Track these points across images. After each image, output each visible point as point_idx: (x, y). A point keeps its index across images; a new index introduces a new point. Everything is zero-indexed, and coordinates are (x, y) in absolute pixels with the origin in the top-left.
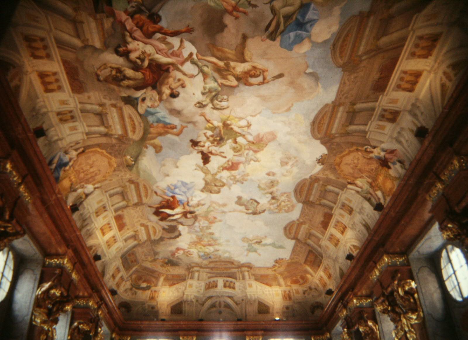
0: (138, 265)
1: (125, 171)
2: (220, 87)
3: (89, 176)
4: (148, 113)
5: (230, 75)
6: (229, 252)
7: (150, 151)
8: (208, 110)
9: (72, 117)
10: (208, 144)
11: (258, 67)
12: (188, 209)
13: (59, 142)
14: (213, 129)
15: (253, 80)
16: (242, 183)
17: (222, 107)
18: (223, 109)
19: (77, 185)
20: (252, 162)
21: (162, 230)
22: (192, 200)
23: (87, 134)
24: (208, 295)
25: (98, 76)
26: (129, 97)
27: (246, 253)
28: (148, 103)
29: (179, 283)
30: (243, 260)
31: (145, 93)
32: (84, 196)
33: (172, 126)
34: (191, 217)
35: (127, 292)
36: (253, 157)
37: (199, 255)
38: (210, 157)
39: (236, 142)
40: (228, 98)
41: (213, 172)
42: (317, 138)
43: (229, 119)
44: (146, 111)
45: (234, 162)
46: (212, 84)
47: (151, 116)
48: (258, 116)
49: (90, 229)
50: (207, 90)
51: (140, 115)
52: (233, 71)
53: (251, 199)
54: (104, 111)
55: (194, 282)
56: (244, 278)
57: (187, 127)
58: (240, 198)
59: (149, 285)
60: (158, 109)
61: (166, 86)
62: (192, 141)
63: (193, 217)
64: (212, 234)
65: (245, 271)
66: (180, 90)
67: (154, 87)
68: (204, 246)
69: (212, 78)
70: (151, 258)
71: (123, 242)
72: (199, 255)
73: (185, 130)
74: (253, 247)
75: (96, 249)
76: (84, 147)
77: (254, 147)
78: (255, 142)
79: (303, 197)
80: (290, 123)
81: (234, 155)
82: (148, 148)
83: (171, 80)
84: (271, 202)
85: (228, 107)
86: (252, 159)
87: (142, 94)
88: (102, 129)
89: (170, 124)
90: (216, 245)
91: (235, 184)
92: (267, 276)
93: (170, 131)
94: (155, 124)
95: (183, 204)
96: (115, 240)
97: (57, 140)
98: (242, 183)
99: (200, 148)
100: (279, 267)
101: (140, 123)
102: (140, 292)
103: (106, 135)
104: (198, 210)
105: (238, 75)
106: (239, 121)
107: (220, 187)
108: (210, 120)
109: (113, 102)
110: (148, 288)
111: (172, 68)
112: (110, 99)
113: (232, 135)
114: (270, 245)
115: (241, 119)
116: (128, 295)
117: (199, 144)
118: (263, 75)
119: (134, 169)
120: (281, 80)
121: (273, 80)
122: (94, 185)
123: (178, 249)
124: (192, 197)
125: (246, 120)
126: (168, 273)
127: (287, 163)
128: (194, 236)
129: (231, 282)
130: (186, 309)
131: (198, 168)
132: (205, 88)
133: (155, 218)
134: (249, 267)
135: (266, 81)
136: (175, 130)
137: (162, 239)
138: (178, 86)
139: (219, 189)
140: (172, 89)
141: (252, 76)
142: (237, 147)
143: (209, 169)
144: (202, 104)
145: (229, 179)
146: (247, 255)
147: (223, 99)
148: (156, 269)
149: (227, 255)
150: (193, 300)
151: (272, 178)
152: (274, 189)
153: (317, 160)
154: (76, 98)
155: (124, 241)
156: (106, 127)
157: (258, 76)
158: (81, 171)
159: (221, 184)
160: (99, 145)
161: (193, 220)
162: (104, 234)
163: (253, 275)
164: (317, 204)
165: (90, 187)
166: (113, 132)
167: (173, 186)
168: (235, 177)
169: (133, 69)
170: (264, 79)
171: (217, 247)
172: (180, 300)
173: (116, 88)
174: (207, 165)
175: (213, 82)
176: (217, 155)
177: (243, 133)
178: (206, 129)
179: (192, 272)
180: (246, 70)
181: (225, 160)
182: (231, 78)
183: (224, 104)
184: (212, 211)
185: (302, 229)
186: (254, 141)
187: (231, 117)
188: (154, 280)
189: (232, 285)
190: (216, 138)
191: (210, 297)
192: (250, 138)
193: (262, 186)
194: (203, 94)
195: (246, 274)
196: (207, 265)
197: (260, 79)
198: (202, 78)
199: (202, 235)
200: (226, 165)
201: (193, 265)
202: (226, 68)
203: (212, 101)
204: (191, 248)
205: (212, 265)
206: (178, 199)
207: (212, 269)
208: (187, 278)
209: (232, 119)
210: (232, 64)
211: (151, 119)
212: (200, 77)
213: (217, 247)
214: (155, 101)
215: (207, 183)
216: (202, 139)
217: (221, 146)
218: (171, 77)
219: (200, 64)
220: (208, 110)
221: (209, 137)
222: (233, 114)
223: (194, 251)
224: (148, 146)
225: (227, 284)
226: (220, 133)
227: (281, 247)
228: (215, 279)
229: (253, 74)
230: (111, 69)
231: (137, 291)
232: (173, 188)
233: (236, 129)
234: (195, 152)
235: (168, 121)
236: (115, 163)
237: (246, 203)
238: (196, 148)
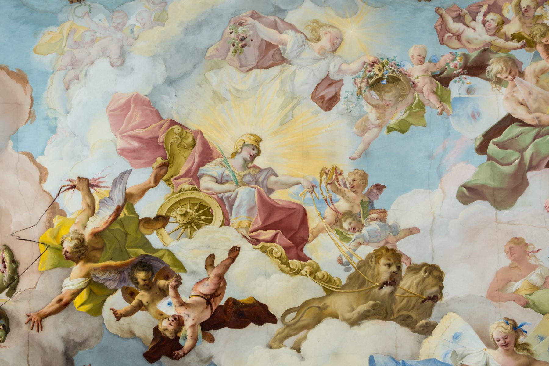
16: (380, 187)
17: (5, 267)
18: (13, 261)
36: (238, 161)
38: (232, 302)
43: (55, 243)
45: (260, 223)
48: (40, 160)
53: (482, 149)
78: (160, 160)
80: (74, 64)
81: (226, 222)
85: (8, 248)
86: (247, 164)
99: (187, 330)
106: (63, 214)
107: (404, 267)
108: (60, 301)
113: (126, 234)
125: (58, 194)
131: (290, 341)
139: (414, 269)
142: (185, 215)
145: (353, 236)
174: (276, 310)
176: (221, 278)
177: (118, 199)
178: (97, 311)
186: (155, 165)
187: (48, 237)
190: (141, 283)
200: (278, 249)
209: (55, 238)
217: (182, 267)
221: (135, 302)
222: (35, 233)
226: (118, 270)
234: (205, 347)
238: (187, 344)
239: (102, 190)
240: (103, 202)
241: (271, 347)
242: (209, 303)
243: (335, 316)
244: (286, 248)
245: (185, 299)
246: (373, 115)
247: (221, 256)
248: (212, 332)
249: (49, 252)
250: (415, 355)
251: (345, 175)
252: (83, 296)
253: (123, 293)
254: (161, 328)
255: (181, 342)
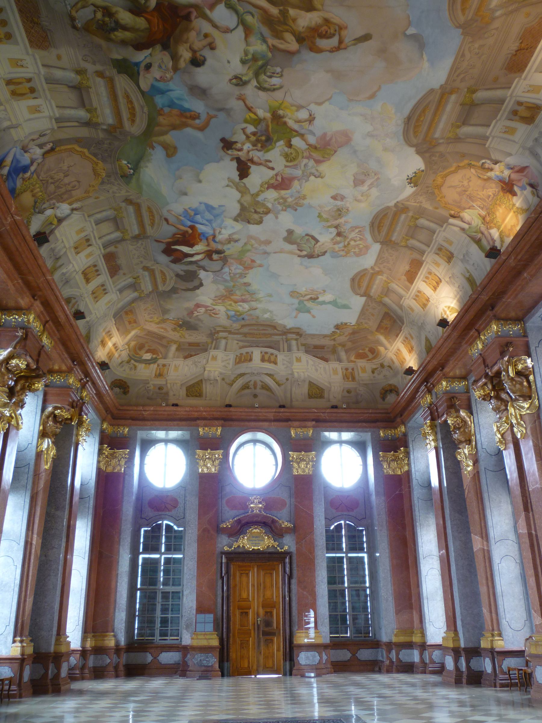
0: (139, 328)
1: (119, 184)
2: (271, 52)
3: (63, 190)
4: (156, 90)
5: (287, 31)
6: (271, 312)
7: (158, 154)
8: (250, 91)
9: (32, 90)
10: (247, 146)
11: (332, 20)
12: (214, 246)
13: (13, 131)
14: (257, 122)
15: (323, 43)
18: (274, 90)
19: (44, 203)
20: (312, 178)
21: (174, 278)
22: (220, 232)
23: (58, 120)
24: (239, 372)
25: (73, 19)
26: (125, 60)
27: (294, 314)
28: (156, 73)
29: (198, 354)
30: (289, 323)
31: (151, 54)
32: (55, 222)
33: (193, 113)
34: (218, 258)
35: (123, 366)
36: (313, 171)
37: (227, 315)
38: (249, 167)
39: (290, 146)
40: (282, 72)
41: (253, 191)
42: (411, 145)
44: (153, 86)
45: (284, 176)
46: (258, 47)
47: (160, 96)
48: (327, 103)
49: (67, 273)
50: (250, 57)
51: (143, 93)
52: (293, 26)
53: (307, 235)
54: (84, 82)
55: (220, 354)
56: (289, 350)
57: (215, 116)
58: (290, 232)
59: (154, 356)
60: (171, 85)
61: (185, 45)
62: (223, 140)
63: (221, 259)
64: (247, 284)
65: (292, 339)
66: (207, 53)
67: (165, 47)
68: (236, 302)
69: (259, 36)
70: (157, 318)
71: (116, 293)
72: (227, 315)
73: (213, 120)
74: (305, 305)
75: (77, 302)
76: (53, 142)
77: (315, 155)
78: (319, 146)
79: (383, 233)
81: (286, 166)
82: (155, 150)
83: (192, 35)
84: (335, 240)
85: (281, 87)
87: (146, 57)
88: (82, 113)
89: (189, 110)
90: (253, 301)
91: (285, 210)
92: (322, 347)
93: (190, 122)
94: (167, 110)
95: (207, 239)
96: (105, 290)
97: (9, 128)
98: (296, 210)
99: (236, 153)
100: (340, 335)
101: (142, 107)
102: (141, 367)
103: (88, 124)
104: (229, 249)
105: (300, 33)
106: (297, 111)
108: (252, 107)
109: (99, 67)
110: (153, 361)
111: (195, 14)
112: (94, 63)
114: (329, 303)
115: (300, 107)
116: (124, 370)
117: (234, 146)
118: (340, 35)
119: (134, 180)
120: (367, 44)
121: (355, 44)
122: (70, 204)
123: (198, 306)
124: (221, 228)
126: (183, 340)
127: (363, 182)
128: (221, 287)
129: (272, 354)
130: (208, 390)
131: (231, 184)
132: (246, 53)
133: (164, 259)
134: (298, 333)
135: (343, 46)
136: (197, 121)
137: (174, 290)
138: (204, 47)
140: (194, 52)
141: (322, 36)
142: (291, 153)
143: (247, 185)
144: (241, 79)
145: (276, 202)
146: (296, 317)
147: (274, 73)
148: (165, 334)
149: (266, 316)
150: (218, 378)
151: (339, 203)
152: (342, 221)
153: (407, 179)
154: (37, 57)
155: (118, 292)
156: (88, 111)
157: (331, 36)
158: (50, 181)
159: (265, 210)
160: (78, 141)
161: (220, 263)
162: (88, 280)
163: (303, 345)
164: (402, 246)
165: (64, 208)
166: (100, 120)
167: (193, 210)
168: (285, 200)
169: (131, 11)
170: (341, 42)
171: (254, 304)
172: (199, 379)
173: (103, 43)
174: (245, 180)
175: (259, 42)
176: (260, 164)
177: (302, 131)
178: (246, 121)
179: (217, 339)
180: (313, 24)
181: (272, 173)
182: (289, 37)
183: (275, 81)
184: (249, 251)
185: (377, 282)
186: (317, 145)
188: (162, 349)
189: (272, 358)
190: (260, 138)
191: (242, 375)
192: (312, 140)
193: (324, 216)
194: (243, 62)
195: (294, 343)
196: (238, 330)
197: (334, 41)
198: (243, 35)
199: (234, 286)
201: (218, 329)
202: (282, 19)
203: (257, 75)
204: (216, 305)
205: (245, 330)
206: (199, 231)
207: (245, 335)
208: (209, 347)
210: (292, 12)
211: (159, 100)
212: (240, 32)
213: (254, 304)
214: (167, 70)
215: (243, 208)
216: (240, 137)
218: (193, 29)
219: (240, 9)
220: (250, 91)
221: (250, 135)
223: (221, 309)
224: (154, 144)
225: (266, 357)
226: (267, 130)
227: (345, 307)
228: (249, 350)
229: (324, 33)
230: (95, 8)
231: (136, 364)
232: (192, 213)
233: (291, 123)
234: (228, 158)
235: (186, 105)
236: (102, 171)
237: (298, 241)
238: (230, 152)
239: (307, 126)
240: (301, 126)
241: (228, 178)
242: (249, 160)
243: (242, 197)
244: (273, 184)
245: (251, 153)
246: (327, 209)
247: (270, 165)
248: (235, 161)
249: (277, 104)
250: (225, 217)
251: (303, 201)
252: (254, 117)
253: (255, 132)
254: (237, 144)
255: (230, 150)
